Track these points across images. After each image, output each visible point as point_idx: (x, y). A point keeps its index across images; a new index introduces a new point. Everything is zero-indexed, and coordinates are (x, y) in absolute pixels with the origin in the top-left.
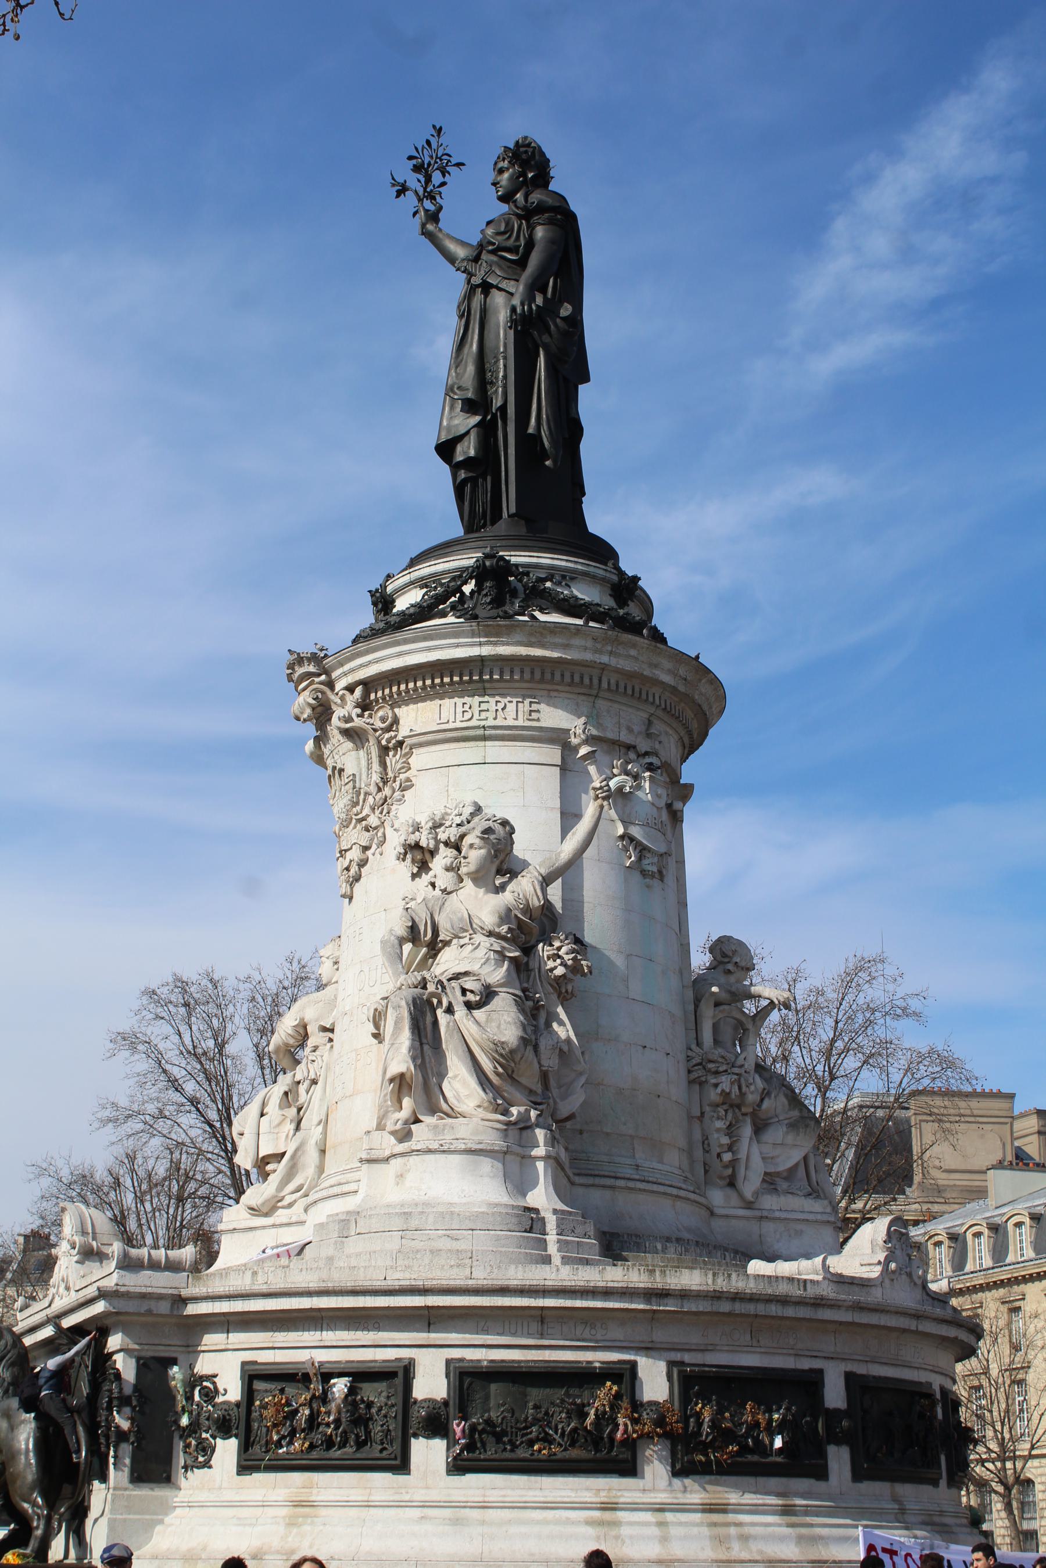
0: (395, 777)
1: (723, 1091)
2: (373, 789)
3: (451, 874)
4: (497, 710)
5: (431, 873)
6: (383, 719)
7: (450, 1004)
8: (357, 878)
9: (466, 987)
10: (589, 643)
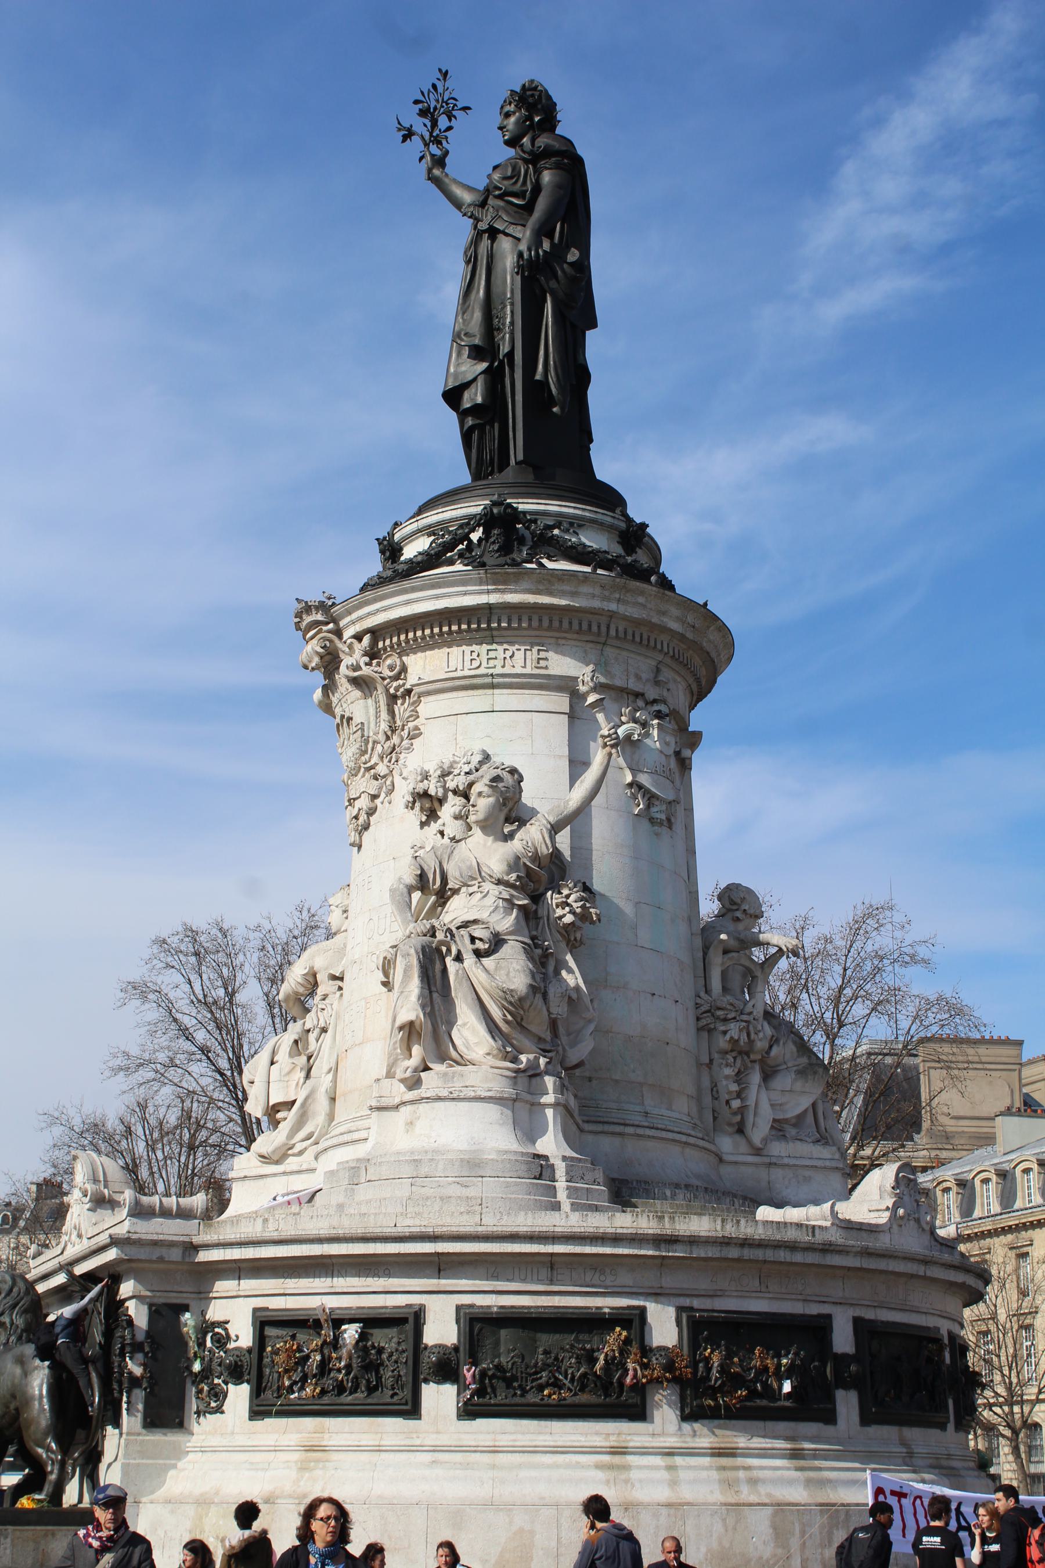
0: (403, 726)
1: (732, 1038)
2: (381, 737)
3: (459, 822)
4: (505, 658)
5: (440, 822)
6: (391, 668)
7: (459, 951)
8: (366, 827)
9: (476, 934)
10: (597, 591)
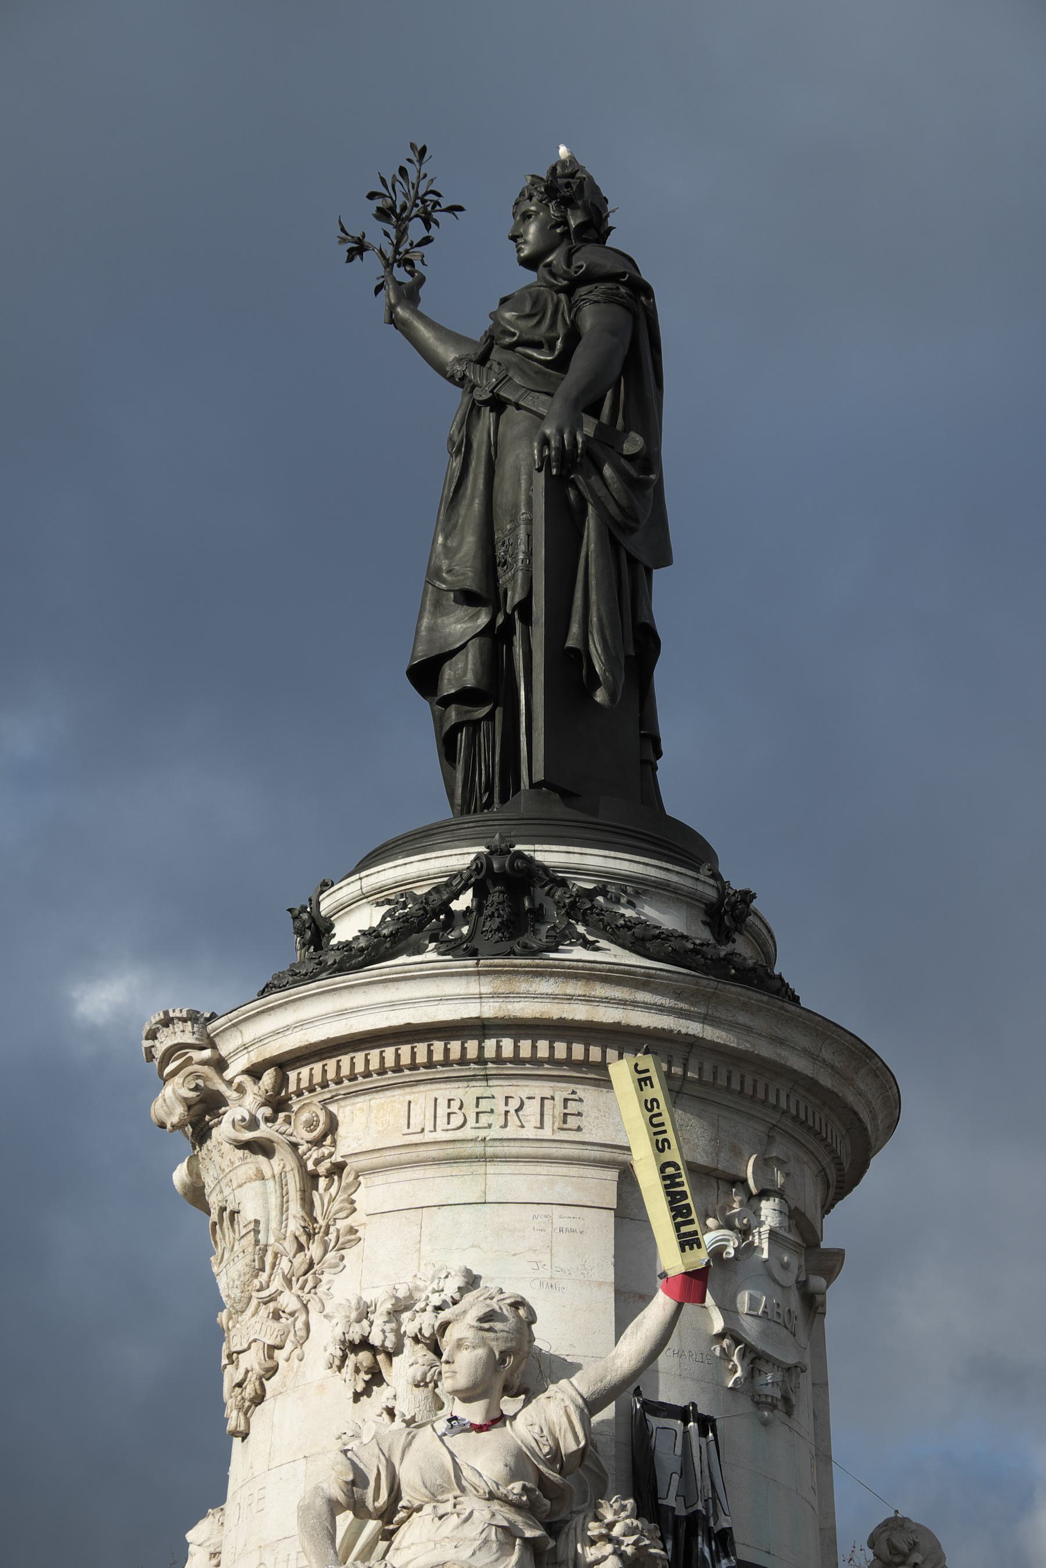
0: (328, 1226)
2: (290, 1246)
3: (421, 1393)
4: (507, 1112)
6: (310, 1125)
8: (259, 1399)
